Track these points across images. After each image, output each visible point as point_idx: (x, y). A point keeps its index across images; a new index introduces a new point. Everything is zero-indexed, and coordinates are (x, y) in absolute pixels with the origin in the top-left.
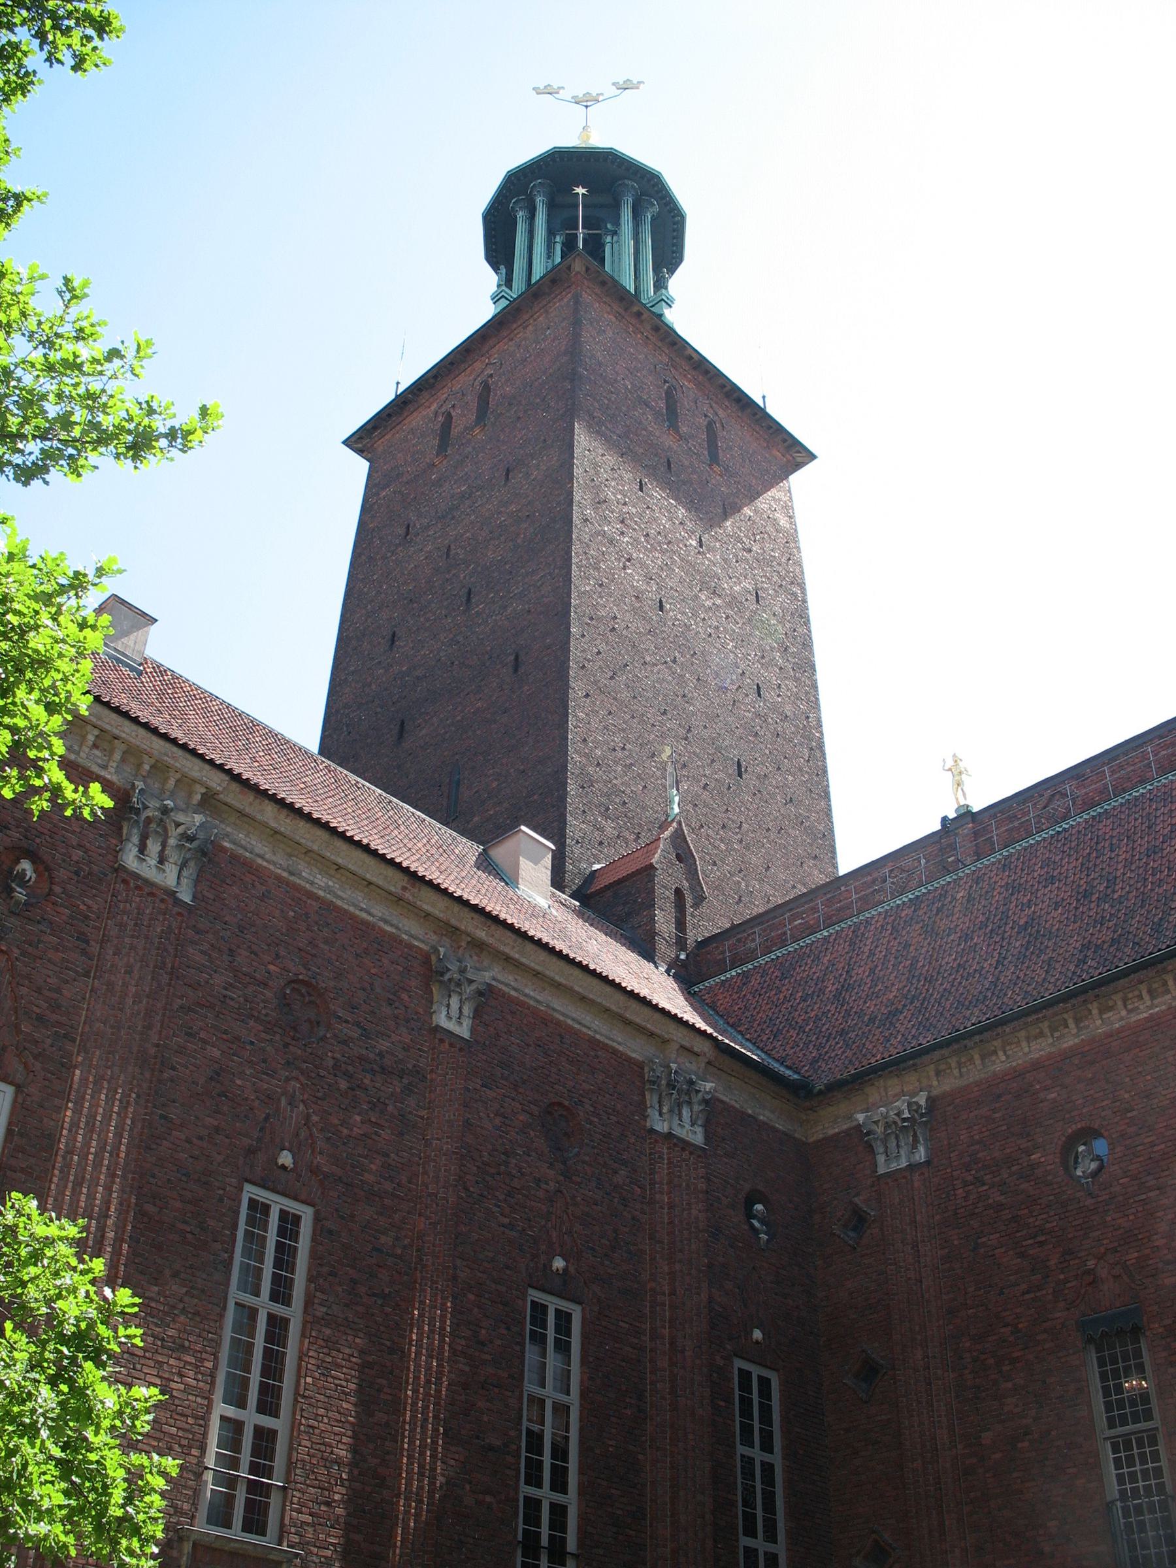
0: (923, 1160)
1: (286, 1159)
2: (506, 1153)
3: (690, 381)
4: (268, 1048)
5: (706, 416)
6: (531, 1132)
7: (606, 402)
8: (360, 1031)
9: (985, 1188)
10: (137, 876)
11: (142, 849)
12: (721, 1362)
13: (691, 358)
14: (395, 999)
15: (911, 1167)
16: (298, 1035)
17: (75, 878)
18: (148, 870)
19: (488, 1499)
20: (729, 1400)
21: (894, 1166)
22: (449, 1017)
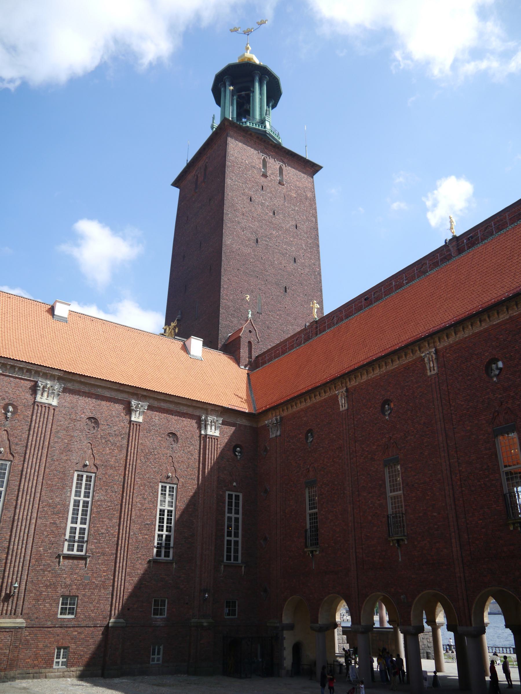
6: (162, 442)
7: (238, 172)
8: (108, 427)
11: (42, 395)
12: (221, 493)
13: (272, 145)
15: (276, 436)
19: (146, 536)
20: (224, 502)
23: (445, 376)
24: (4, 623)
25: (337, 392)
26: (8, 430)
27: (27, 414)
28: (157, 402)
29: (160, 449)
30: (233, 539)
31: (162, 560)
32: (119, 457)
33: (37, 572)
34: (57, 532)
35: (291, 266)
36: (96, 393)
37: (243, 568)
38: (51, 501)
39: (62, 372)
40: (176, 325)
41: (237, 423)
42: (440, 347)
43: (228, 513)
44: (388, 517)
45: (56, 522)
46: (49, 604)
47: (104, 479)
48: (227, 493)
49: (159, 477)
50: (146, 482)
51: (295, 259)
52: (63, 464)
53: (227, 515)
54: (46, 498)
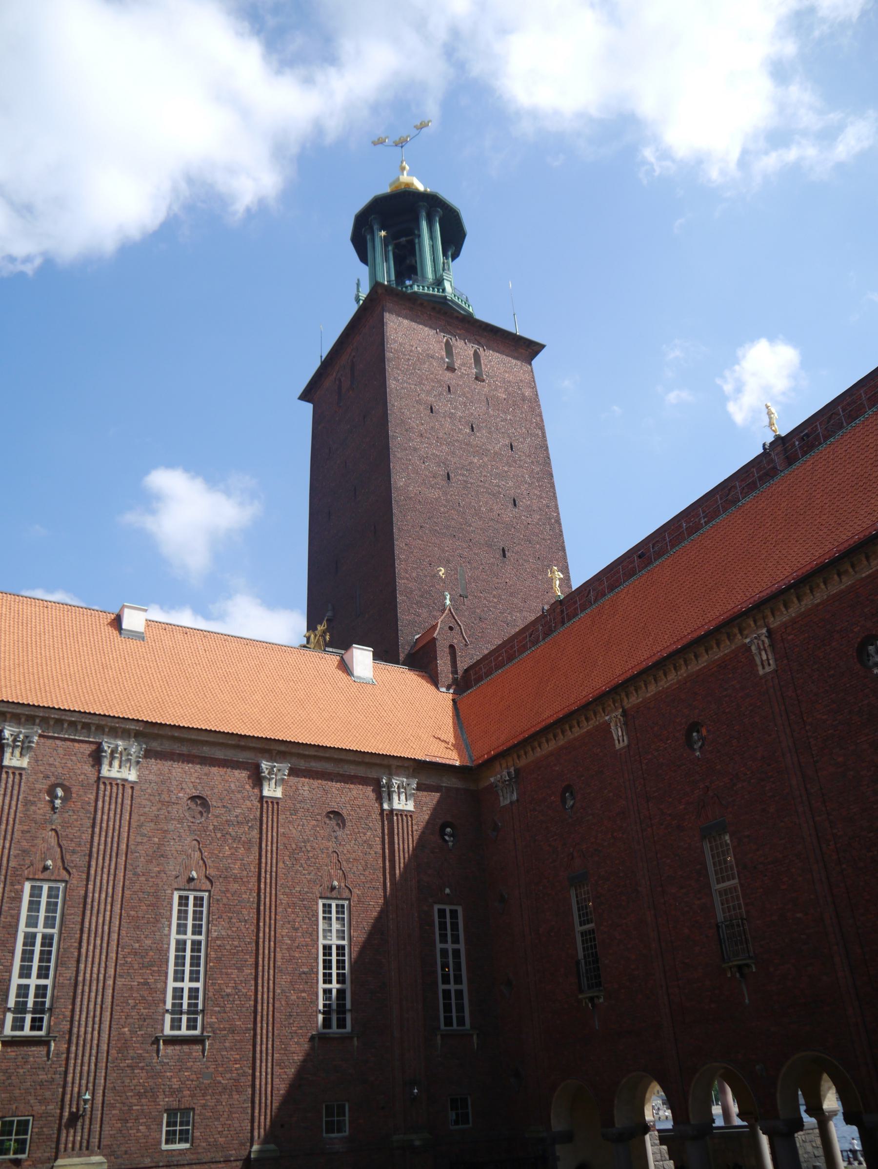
3: (460, 330)
6: (318, 829)
7: (406, 367)
8: (225, 809)
11: (111, 765)
13: (457, 317)
15: (511, 803)
17: (81, 788)
19: (303, 995)
23: (789, 673)
24: (70, 1165)
25: (607, 718)
26: (58, 830)
27: (87, 799)
28: (305, 761)
29: (315, 841)
30: (452, 987)
31: (333, 1033)
33: (121, 1071)
34: (151, 998)
35: (509, 514)
37: (475, 1037)
38: (138, 944)
39: (141, 724)
40: (326, 629)
41: (442, 786)
42: (775, 625)
43: (441, 942)
44: (718, 927)
45: (149, 981)
46: (145, 1127)
47: (225, 900)
48: (436, 907)
49: (317, 890)
50: (296, 899)
51: (514, 501)
52: (154, 880)
53: (439, 946)
54: (128, 941)
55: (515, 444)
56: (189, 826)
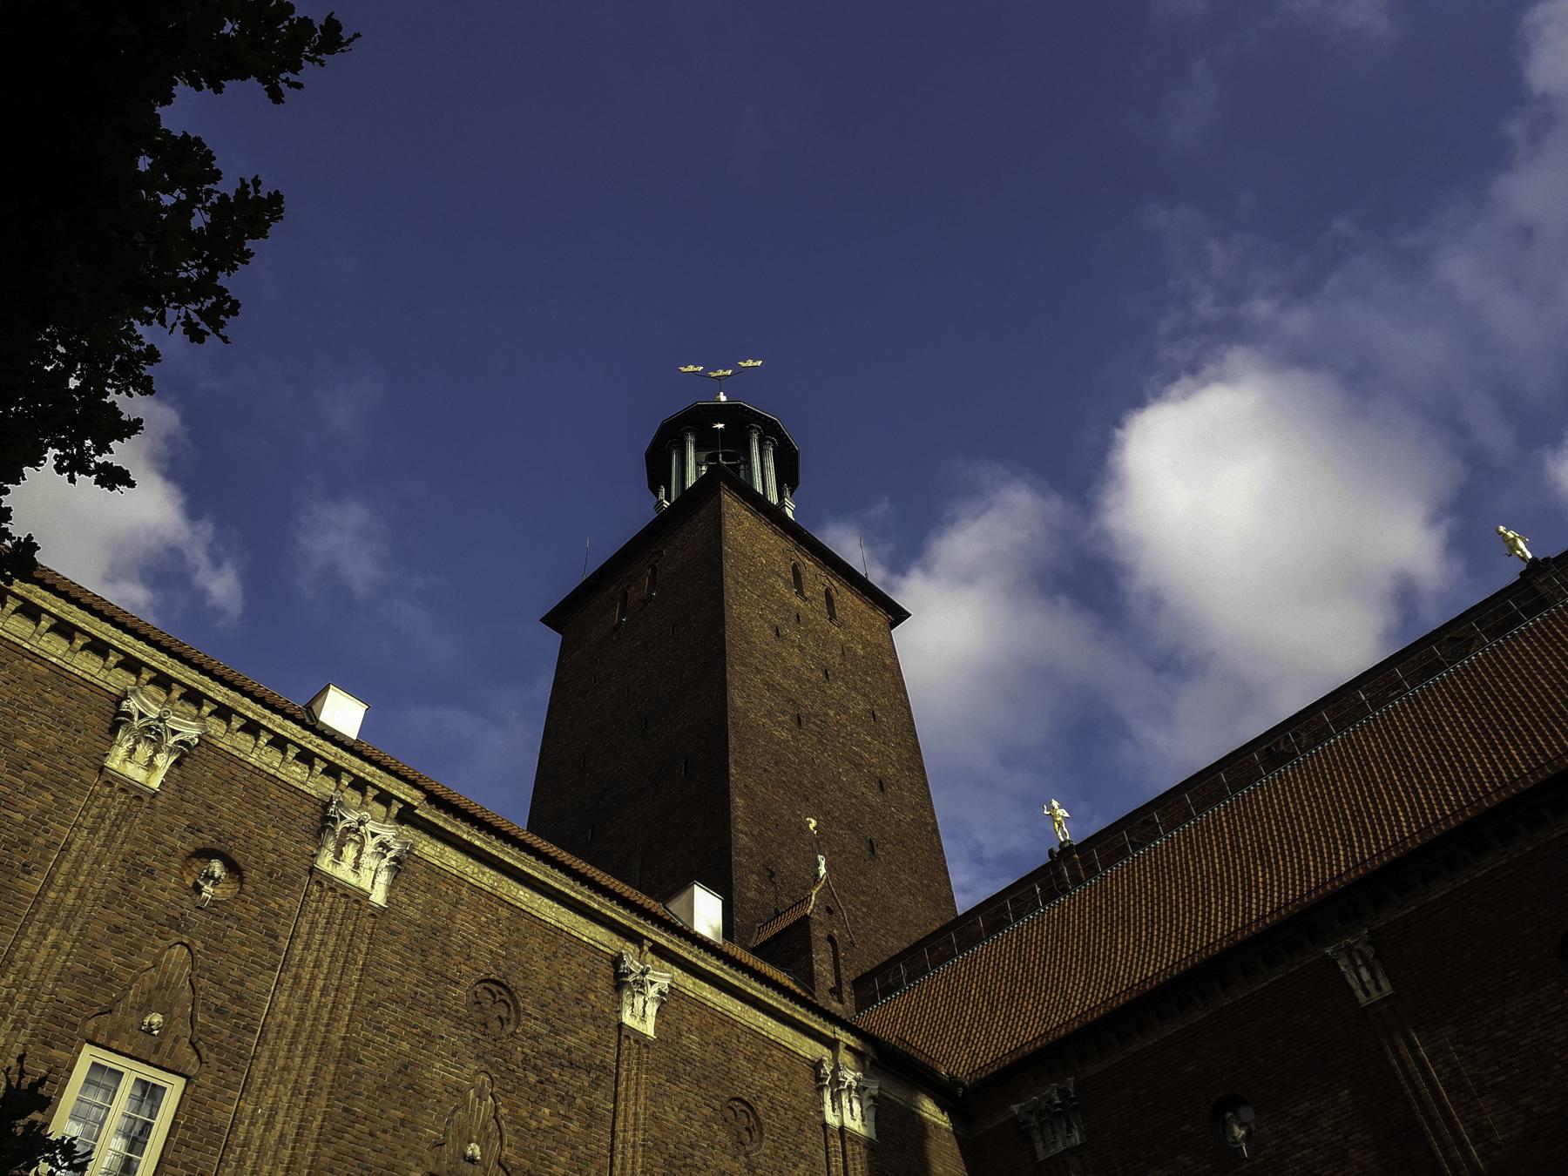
0: (1079, 1142)
1: (474, 1150)
2: (691, 1146)
3: (809, 560)
4: (458, 1043)
5: (824, 585)
7: (747, 572)
8: (549, 1028)
9: (1142, 1164)
10: (330, 878)
11: (338, 854)
14: (582, 998)
15: (1070, 1151)
16: (488, 1031)
18: (344, 872)
21: (1052, 1151)
22: (632, 1015)
27: (273, 905)
28: (694, 984)
32: (584, 1150)
35: (874, 798)
36: (513, 902)
39: (417, 794)
51: (880, 782)
55: (878, 714)
56: (476, 1040)
